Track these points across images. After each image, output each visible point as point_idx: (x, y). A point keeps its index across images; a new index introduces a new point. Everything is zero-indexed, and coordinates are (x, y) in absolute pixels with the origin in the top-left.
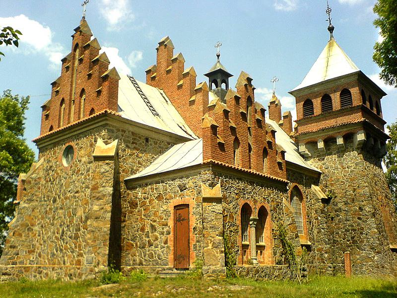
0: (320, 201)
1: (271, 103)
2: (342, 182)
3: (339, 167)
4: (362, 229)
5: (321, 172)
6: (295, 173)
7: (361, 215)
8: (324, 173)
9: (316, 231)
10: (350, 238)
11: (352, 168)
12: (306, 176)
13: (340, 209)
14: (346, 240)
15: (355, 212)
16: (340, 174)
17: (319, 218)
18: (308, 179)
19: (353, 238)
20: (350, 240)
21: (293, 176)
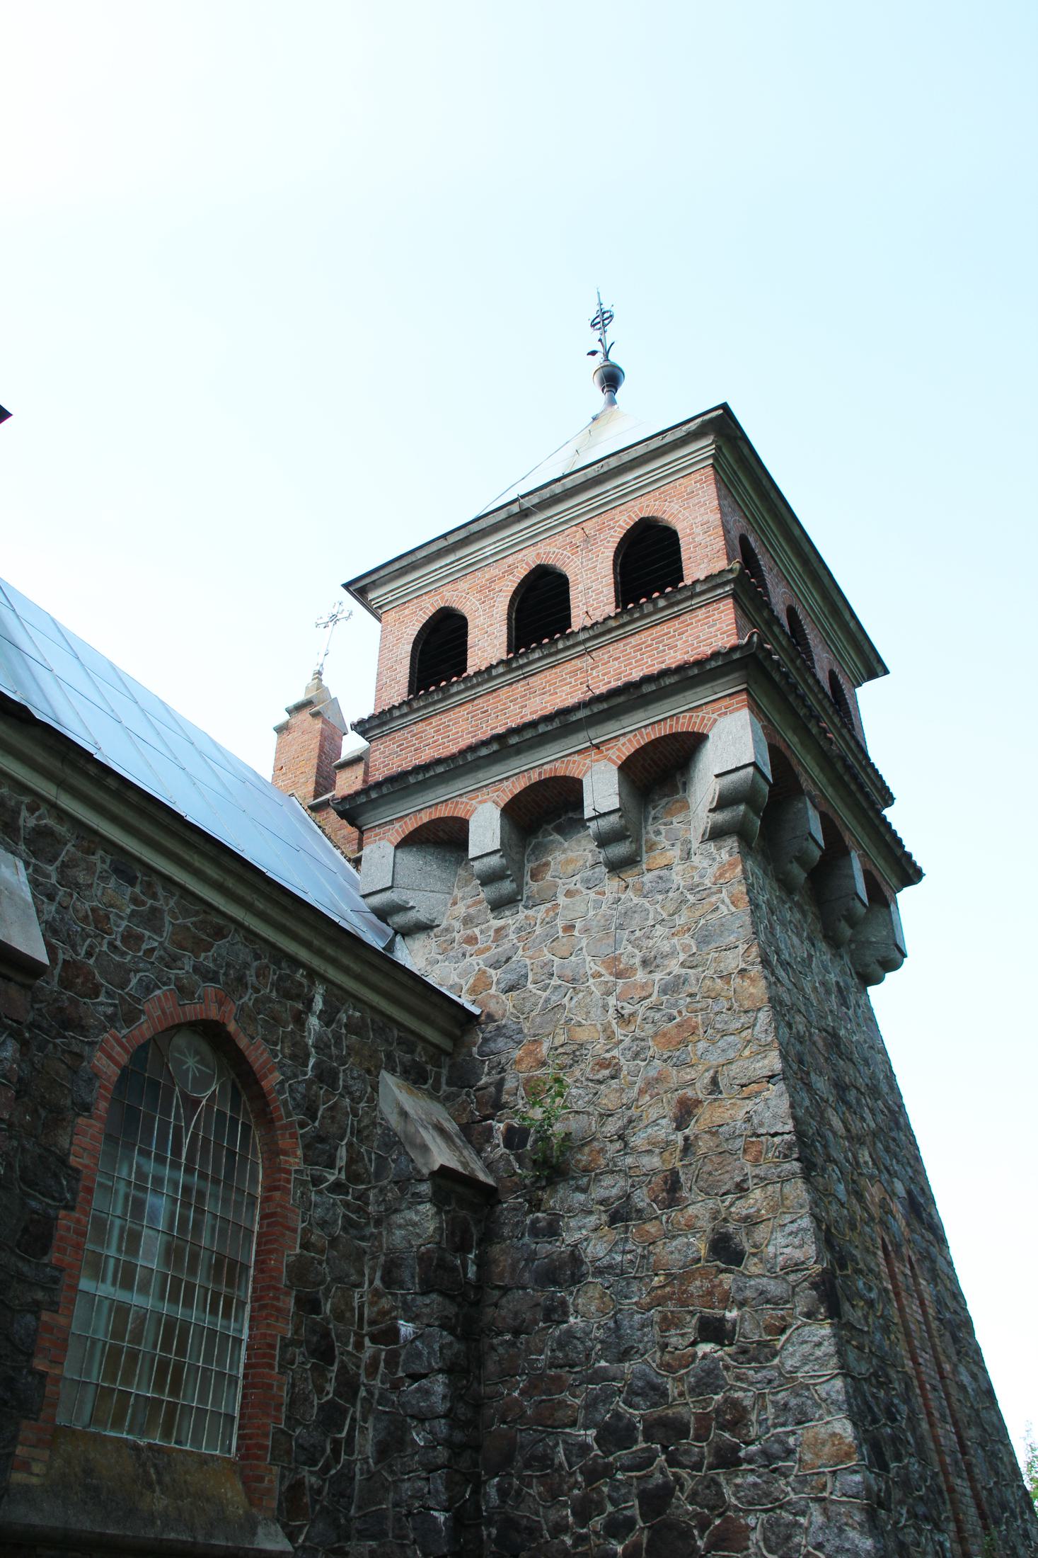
0: (425, 1188)
1: (299, 708)
2: (603, 1064)
3: (592, 966)
4: (735, 1417)
5: (476, 1010)
6: (219, 933)
7: (727, 1301)
8: (491, 1018)
9: (367, 1443)
10: (633, 1508)
11: (674, 966)
12: (337, 997)
13: (575, 1258)
14: (598, 1522)
15: (687, 1277)
16: (596, 1012)
17: (406, 1329)
18: (352, 1028)
19: (655, 1501)
20: (630, 1524)
21: (200, 946)
